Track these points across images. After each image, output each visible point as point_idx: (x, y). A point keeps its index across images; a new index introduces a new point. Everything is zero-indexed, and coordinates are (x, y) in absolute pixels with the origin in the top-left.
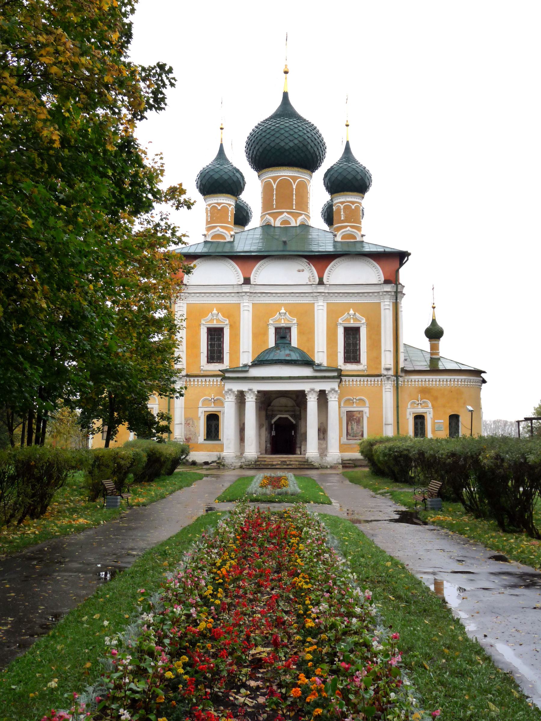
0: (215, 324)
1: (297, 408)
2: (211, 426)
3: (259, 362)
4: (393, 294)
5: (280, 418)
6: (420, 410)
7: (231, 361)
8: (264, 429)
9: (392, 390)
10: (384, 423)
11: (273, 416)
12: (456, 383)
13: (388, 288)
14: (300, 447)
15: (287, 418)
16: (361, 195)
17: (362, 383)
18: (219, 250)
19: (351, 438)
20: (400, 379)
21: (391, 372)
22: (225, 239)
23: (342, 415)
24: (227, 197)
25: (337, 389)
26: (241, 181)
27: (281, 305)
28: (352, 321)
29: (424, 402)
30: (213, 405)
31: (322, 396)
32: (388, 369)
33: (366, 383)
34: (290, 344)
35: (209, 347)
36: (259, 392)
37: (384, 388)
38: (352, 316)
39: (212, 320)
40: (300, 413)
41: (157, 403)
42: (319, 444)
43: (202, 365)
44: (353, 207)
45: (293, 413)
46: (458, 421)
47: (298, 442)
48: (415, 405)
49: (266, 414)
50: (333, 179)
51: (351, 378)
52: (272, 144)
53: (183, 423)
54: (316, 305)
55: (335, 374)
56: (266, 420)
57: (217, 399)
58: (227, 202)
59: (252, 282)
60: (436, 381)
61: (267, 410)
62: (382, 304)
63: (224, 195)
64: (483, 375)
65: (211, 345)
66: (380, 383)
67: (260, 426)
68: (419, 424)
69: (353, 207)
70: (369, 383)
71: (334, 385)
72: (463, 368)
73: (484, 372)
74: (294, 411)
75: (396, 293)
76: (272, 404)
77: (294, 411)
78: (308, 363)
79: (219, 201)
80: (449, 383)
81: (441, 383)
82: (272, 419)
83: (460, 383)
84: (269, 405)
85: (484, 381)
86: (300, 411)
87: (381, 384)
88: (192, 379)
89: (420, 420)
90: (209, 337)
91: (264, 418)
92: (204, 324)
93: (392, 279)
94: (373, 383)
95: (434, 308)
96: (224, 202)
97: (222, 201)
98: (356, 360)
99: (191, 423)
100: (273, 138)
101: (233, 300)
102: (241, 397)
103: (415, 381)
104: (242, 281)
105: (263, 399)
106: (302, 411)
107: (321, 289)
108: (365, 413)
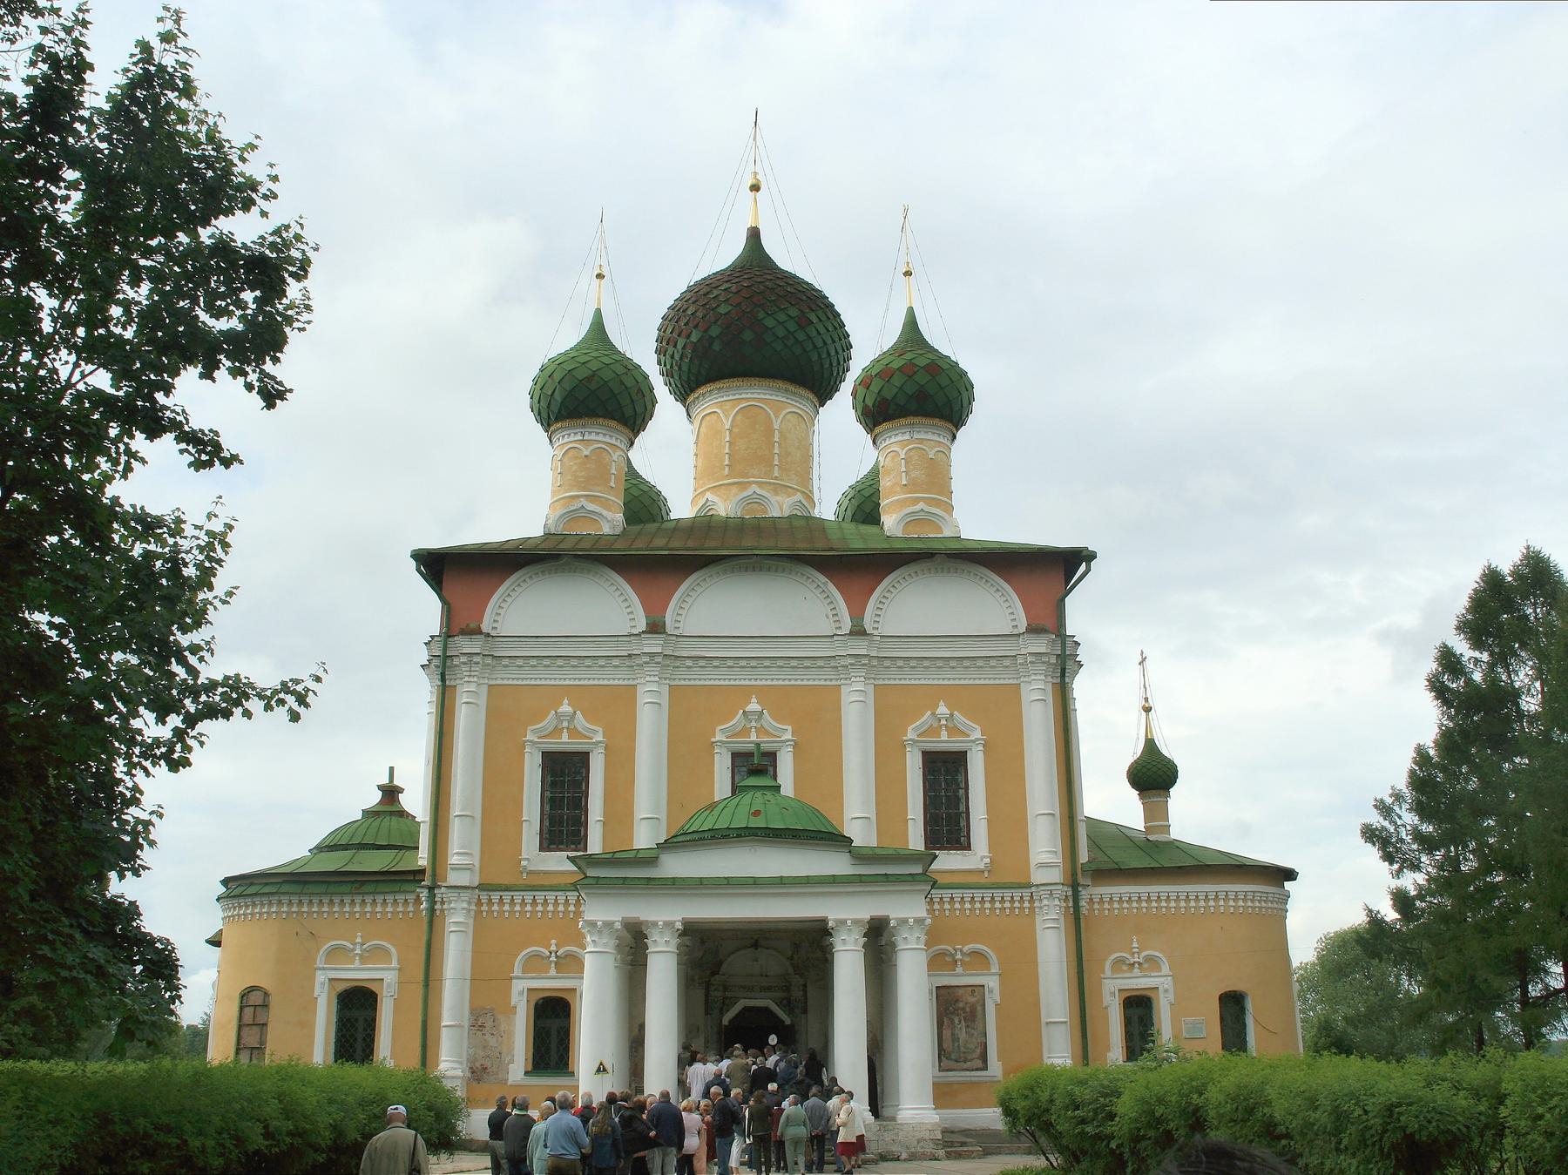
2: (548, 1033)
5: (746, 1009)
6: (1138, 982)
10: (1044, 1020)
11: (725, 1006)
12: (1232, 903)
15: (767, 1010)
17: (978, 905)
19: (953, 1064)
20: (1084, 894)
28: (944, 736)
29: (1149, 959)
30: (553, 972)
33: (987, 905)
35: (547, 808)
37: (1038, 919)
38: (943, 722)
41: (394, 964)
43: (524, 856)
45: (784, 995)
46: (1243, 1010)
48: (1125, 968)
49: (707, 996)
53: (466, 1024)
56: (707, 1013)
60: (1178, 899)
61: (708, 986)
65: (552, 800)
66: (1027, 904)
68: (1136, 1019)
70: (998, 905)
76: (723, 969)
77: (788, 989)
80: (1212, 903)
81: (1192, 904)
83: (1241, 903)
84: (714, 973)
86: (805, 986)
88: (495, 896)
89: (1139, 1008)
90: (549, 779)
91: (701, 1011)
92: (533, 743)
93: (1049, 624)
94: (1007, 905)
98: (958, 841)
99: (489, 1024)
103: (1121, 901)
105: (700, 954)
108: (991, 991)
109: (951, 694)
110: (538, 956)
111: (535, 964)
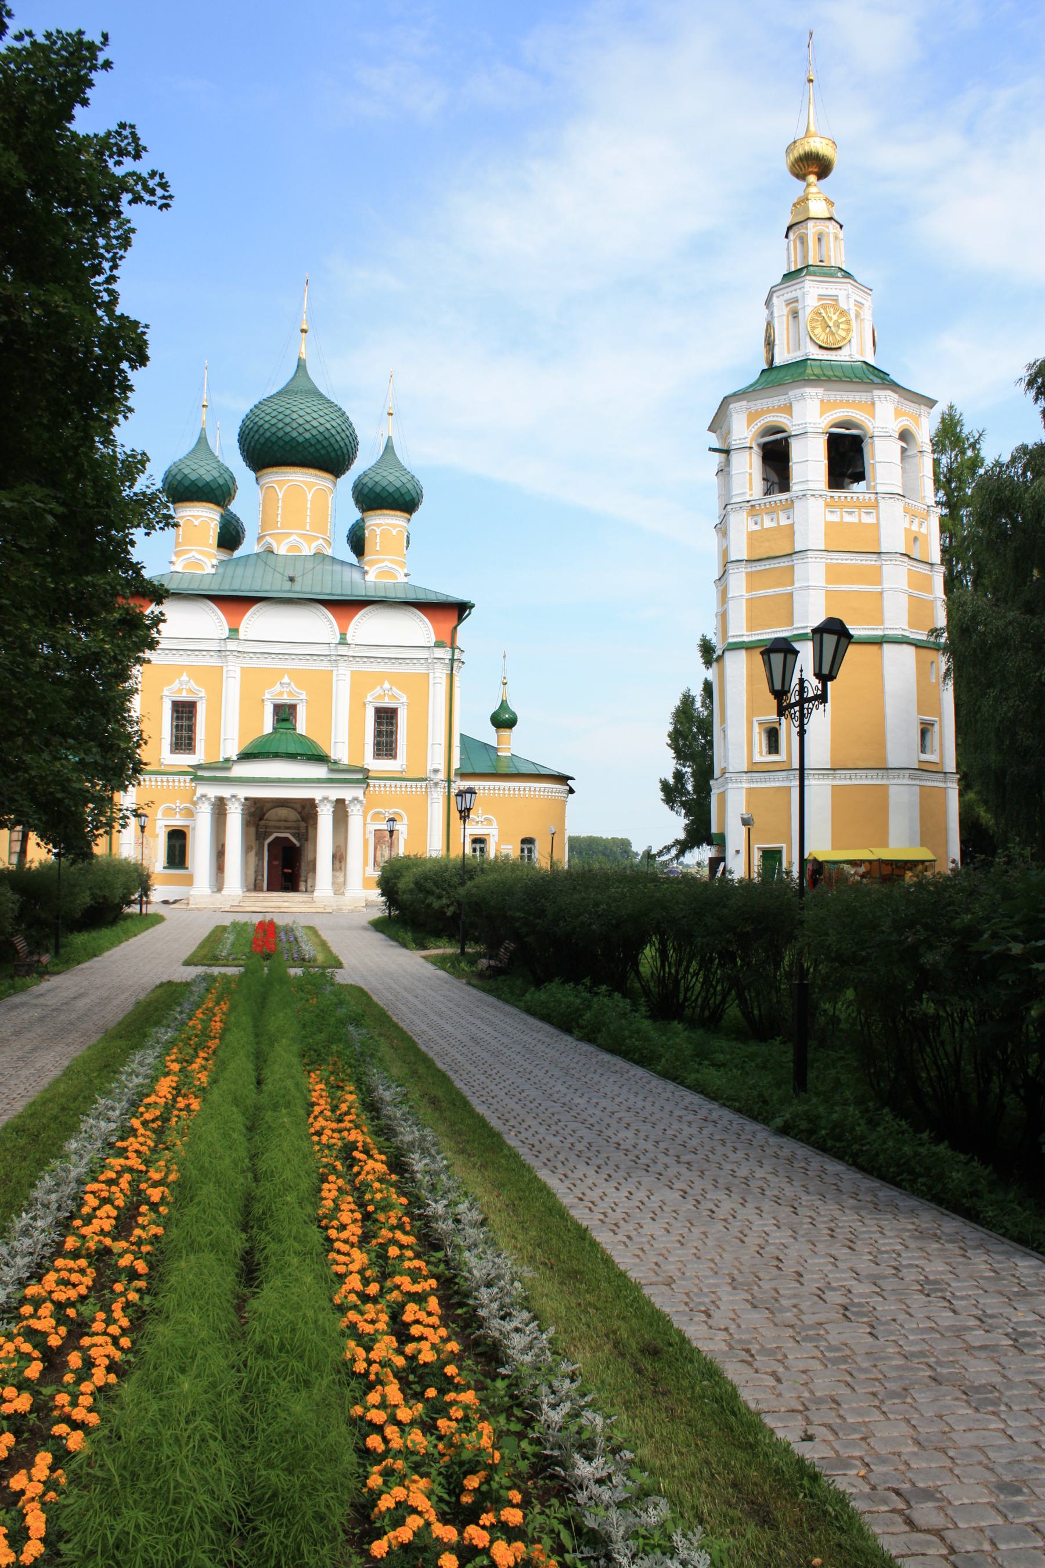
0: (184, 697)
1: (303, 824)
2: (175, 847)
3: (246, 756)
4: (447, 661)
5: (277, 838)
7: (207, 753)
8: (253, 853)
9: (441, 801)
11: (267, 835)
13: (441, 653)
14: (306, 881)
15: (287, 838)
16: (407, 515)
18: (194, 585)
20: (453, 784)
21: (442, 776)
22: (203, 569)
23: (367, 836)
24: (210, 508)
25: (361, 798)
26: (231, 486)
27: (282, 672)
28: (387, 699)
29: (486, 819)
30: (178, 816)
31: (340, 807)
32: (436, 771)
34: (295, 729)
36: (246, 799)
39: (180, 690)
40: (307, 832)
42: (334, 877)
44: (394, 532)
47: (303, 873)
50: (366, 490)
51: (382, 783)
52: (280, 434)
53: (133, 842)
54: (335, 673)
55: (360, 776)
57: (185, 808)
58: (208, 515)
59: (241, 636)
61: (257, 826)
62: (431, 676)
63: (204, 504)
64: (570, 782)
67: (247, 849)
69: (394, 532)
71: (358, 792)
72: (543, 772)
73: (572, 778)
74: (298, 828)
75: (452, 660)
76: (266, 817)
77: (298, 828)
78: (320, 758)
79: (196, 513)
82: (264, 839)
84: (261, 819)
85: (571, 791)
86: (307, 827)
87: (426, 792)
91: (253, 837)
95: (505, 684)
96: (204, 514)
97: (200, 514)
100: (280, 425)
101: (213, 661)
102: (220, 807)
104: (226, 634)
105: (253, 810)
106: (310, 828)
107: (343, 650)
109: (394, 679)
110: (170, 808)
111: (170, 812)
